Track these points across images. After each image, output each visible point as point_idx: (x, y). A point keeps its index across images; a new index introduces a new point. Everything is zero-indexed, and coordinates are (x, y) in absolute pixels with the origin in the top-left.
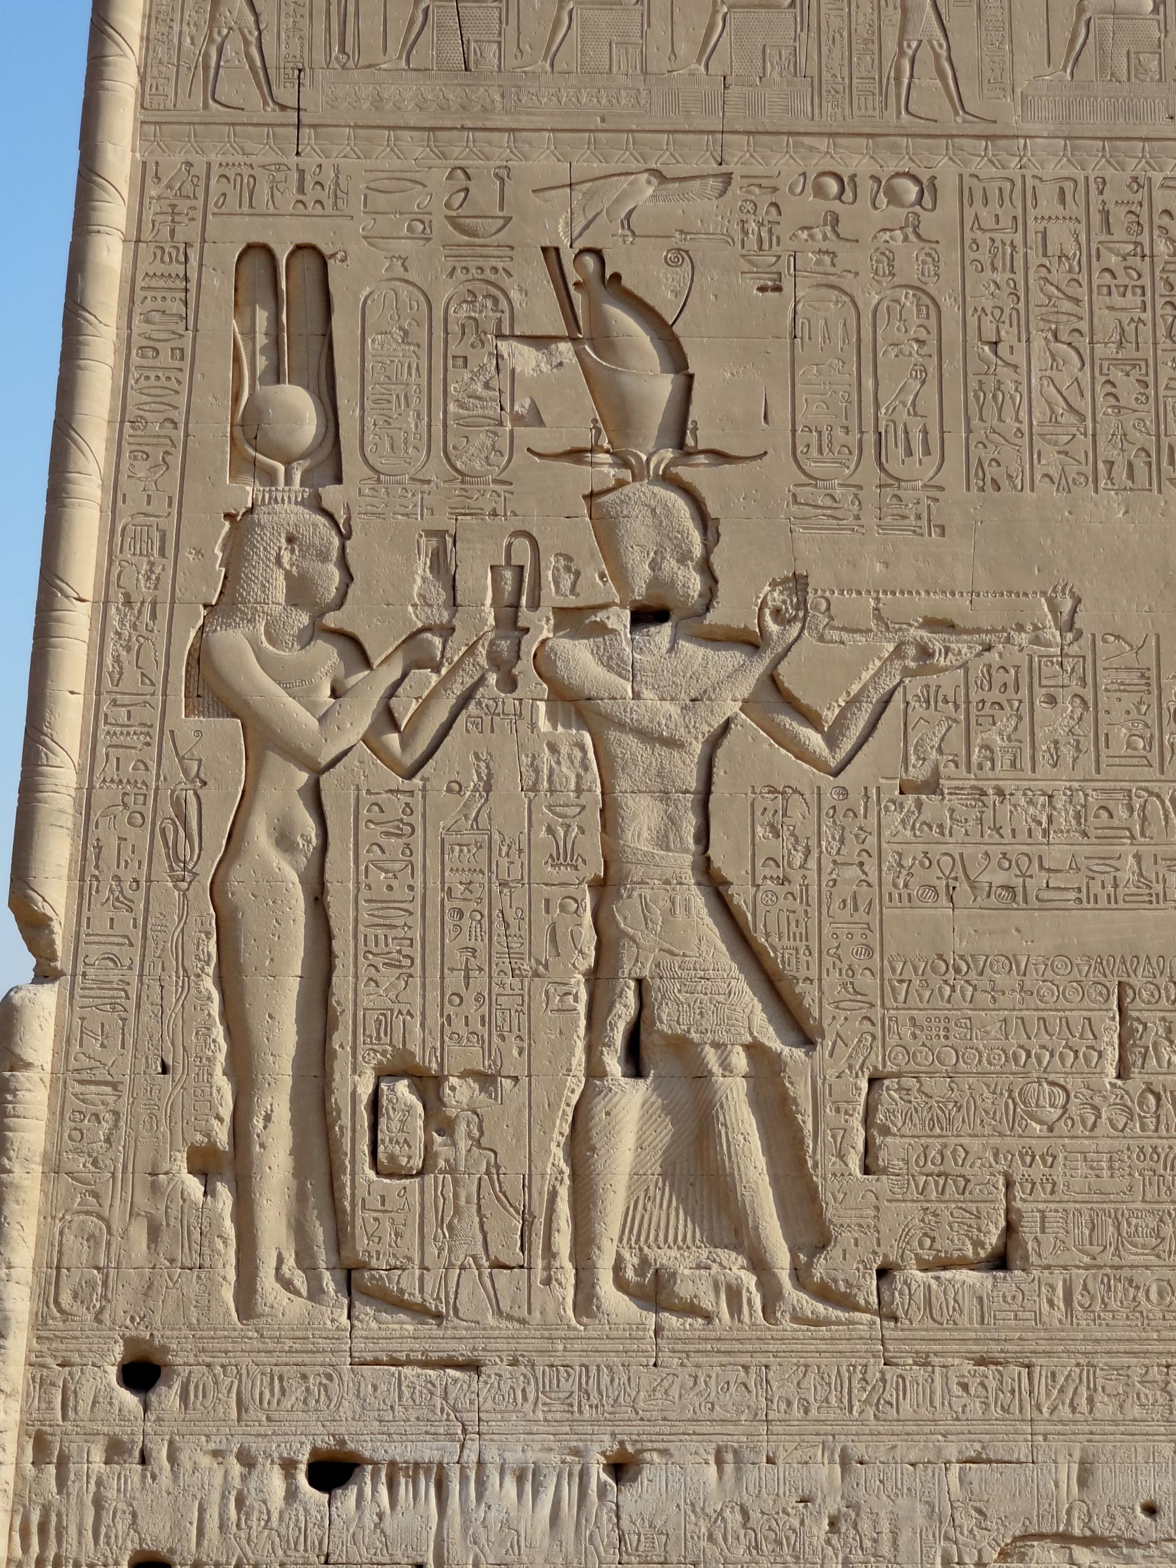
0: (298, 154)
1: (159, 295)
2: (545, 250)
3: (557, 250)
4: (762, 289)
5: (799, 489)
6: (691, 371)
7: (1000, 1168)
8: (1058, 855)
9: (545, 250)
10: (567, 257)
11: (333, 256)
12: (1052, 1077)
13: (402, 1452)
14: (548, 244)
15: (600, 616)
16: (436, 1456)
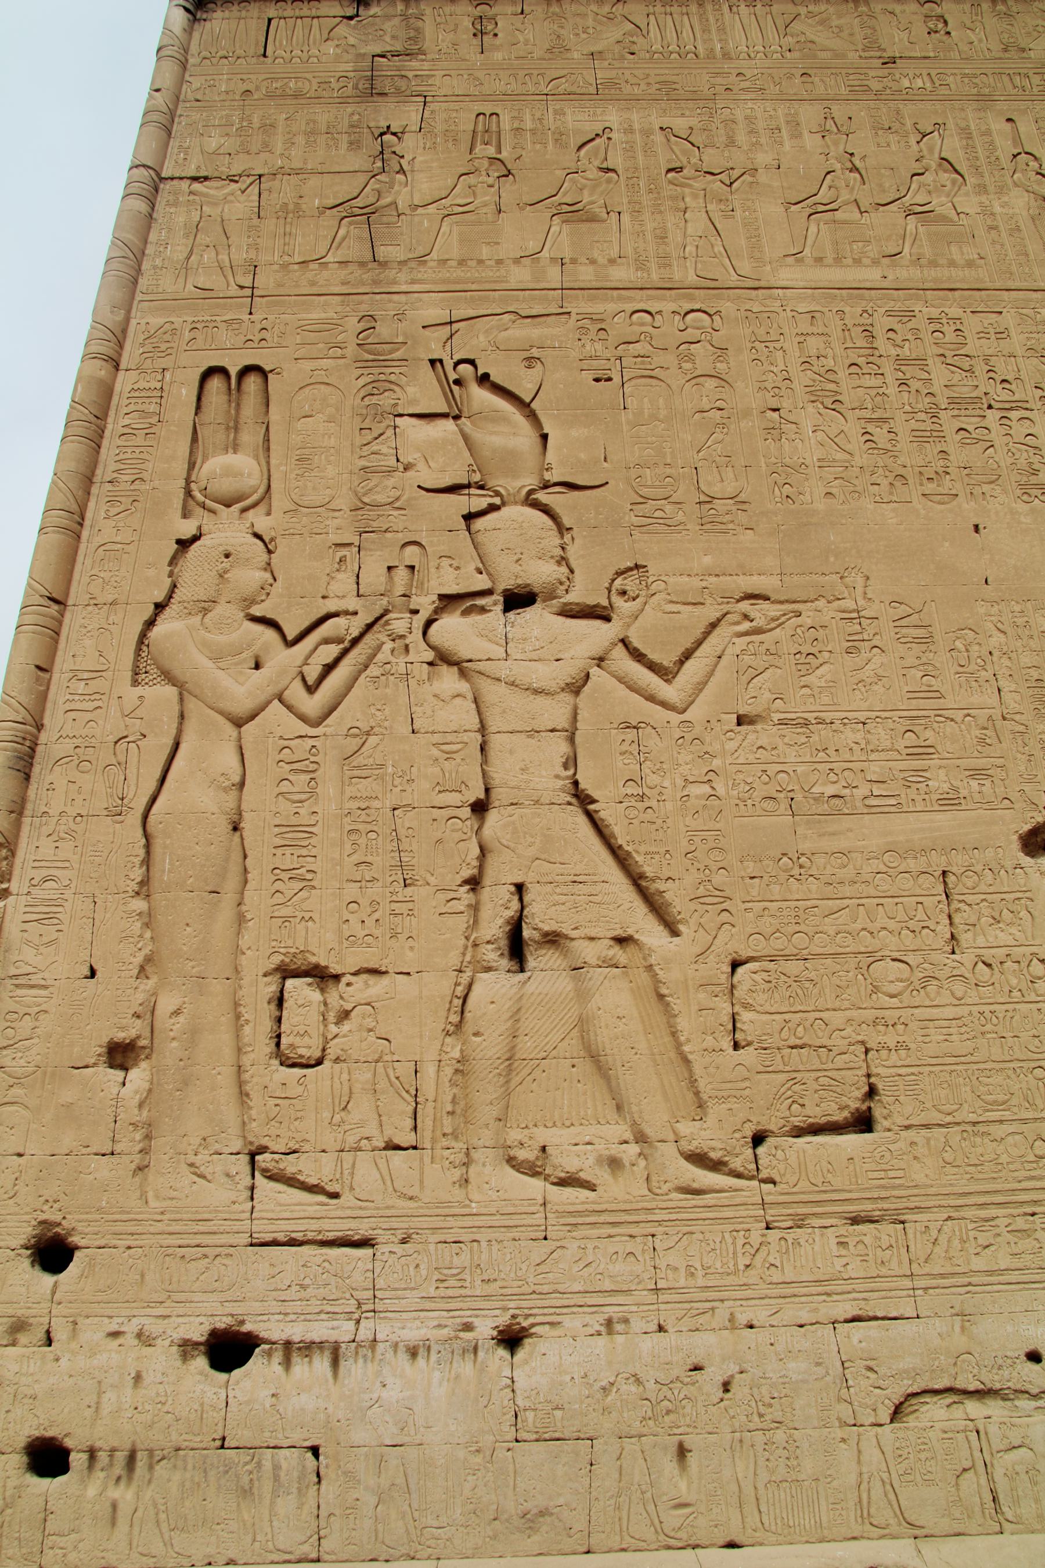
0: (251, 313)
1: (140, 401)
2: (432, 362)
3: (441, 361)
4: (597, 380)
5: (634, 507)
6: (545, 431)
7: (860, 1038)
8: (877, 769)
9: (432, 362)
10: (449, 364)
11: (271, 371)
12: (896, 955)
13: (297, 1332)
14: (435, 356)
15: (480, 602)
16: (332, 1336)
